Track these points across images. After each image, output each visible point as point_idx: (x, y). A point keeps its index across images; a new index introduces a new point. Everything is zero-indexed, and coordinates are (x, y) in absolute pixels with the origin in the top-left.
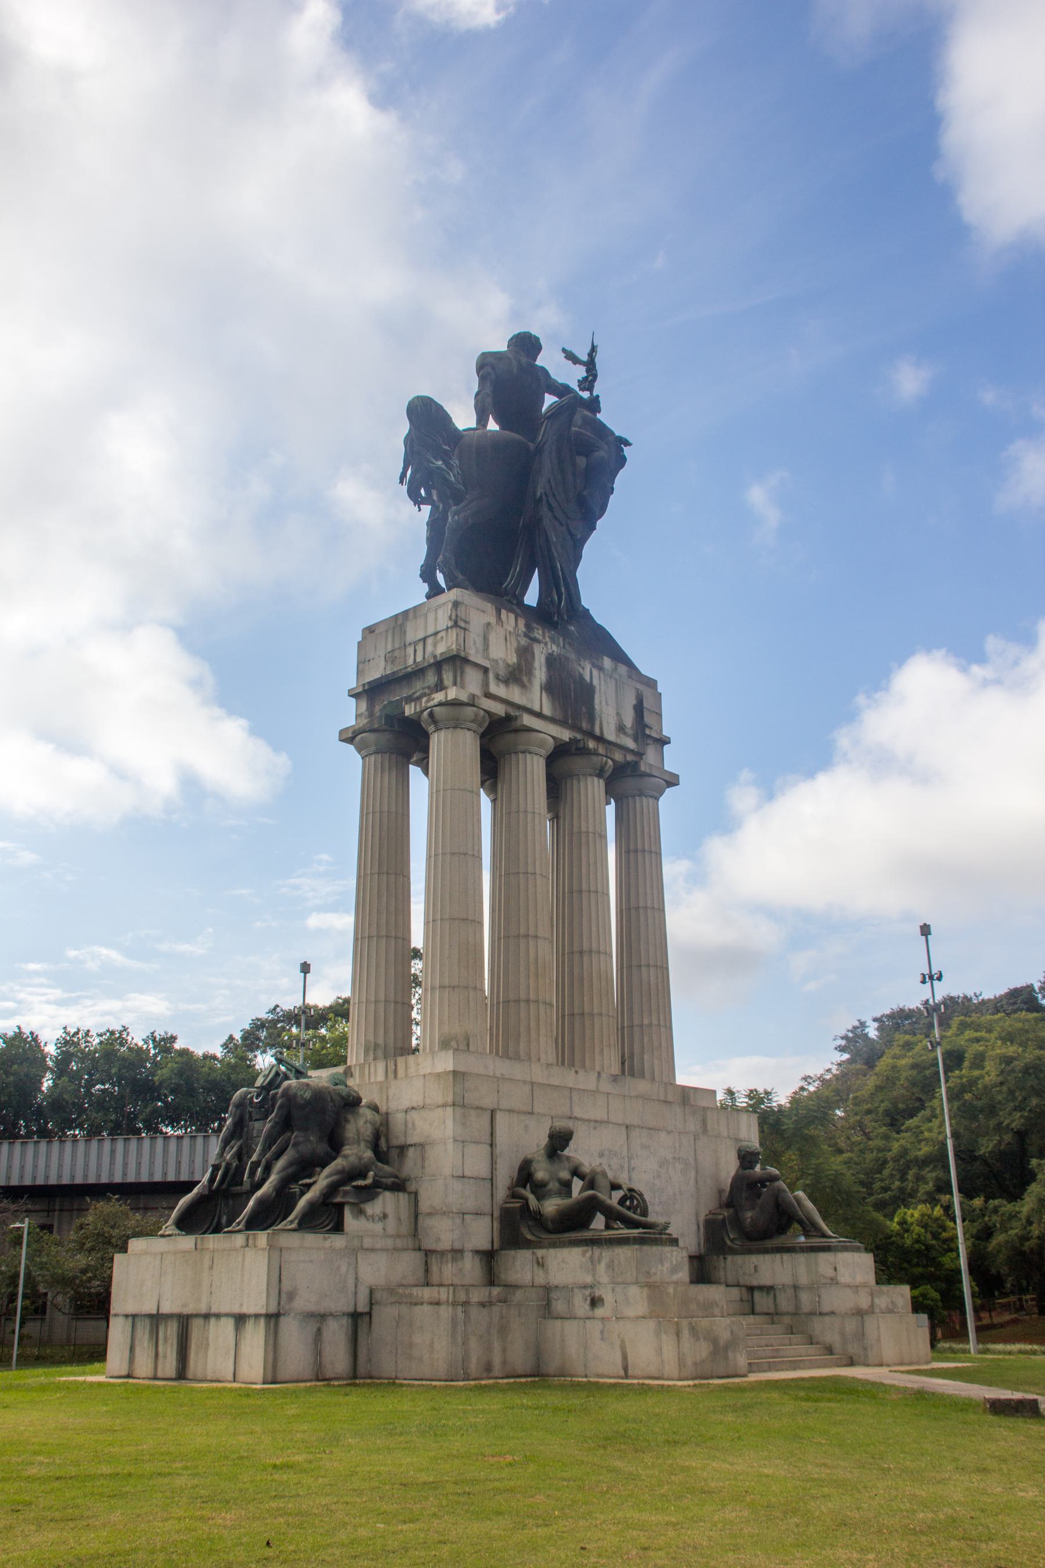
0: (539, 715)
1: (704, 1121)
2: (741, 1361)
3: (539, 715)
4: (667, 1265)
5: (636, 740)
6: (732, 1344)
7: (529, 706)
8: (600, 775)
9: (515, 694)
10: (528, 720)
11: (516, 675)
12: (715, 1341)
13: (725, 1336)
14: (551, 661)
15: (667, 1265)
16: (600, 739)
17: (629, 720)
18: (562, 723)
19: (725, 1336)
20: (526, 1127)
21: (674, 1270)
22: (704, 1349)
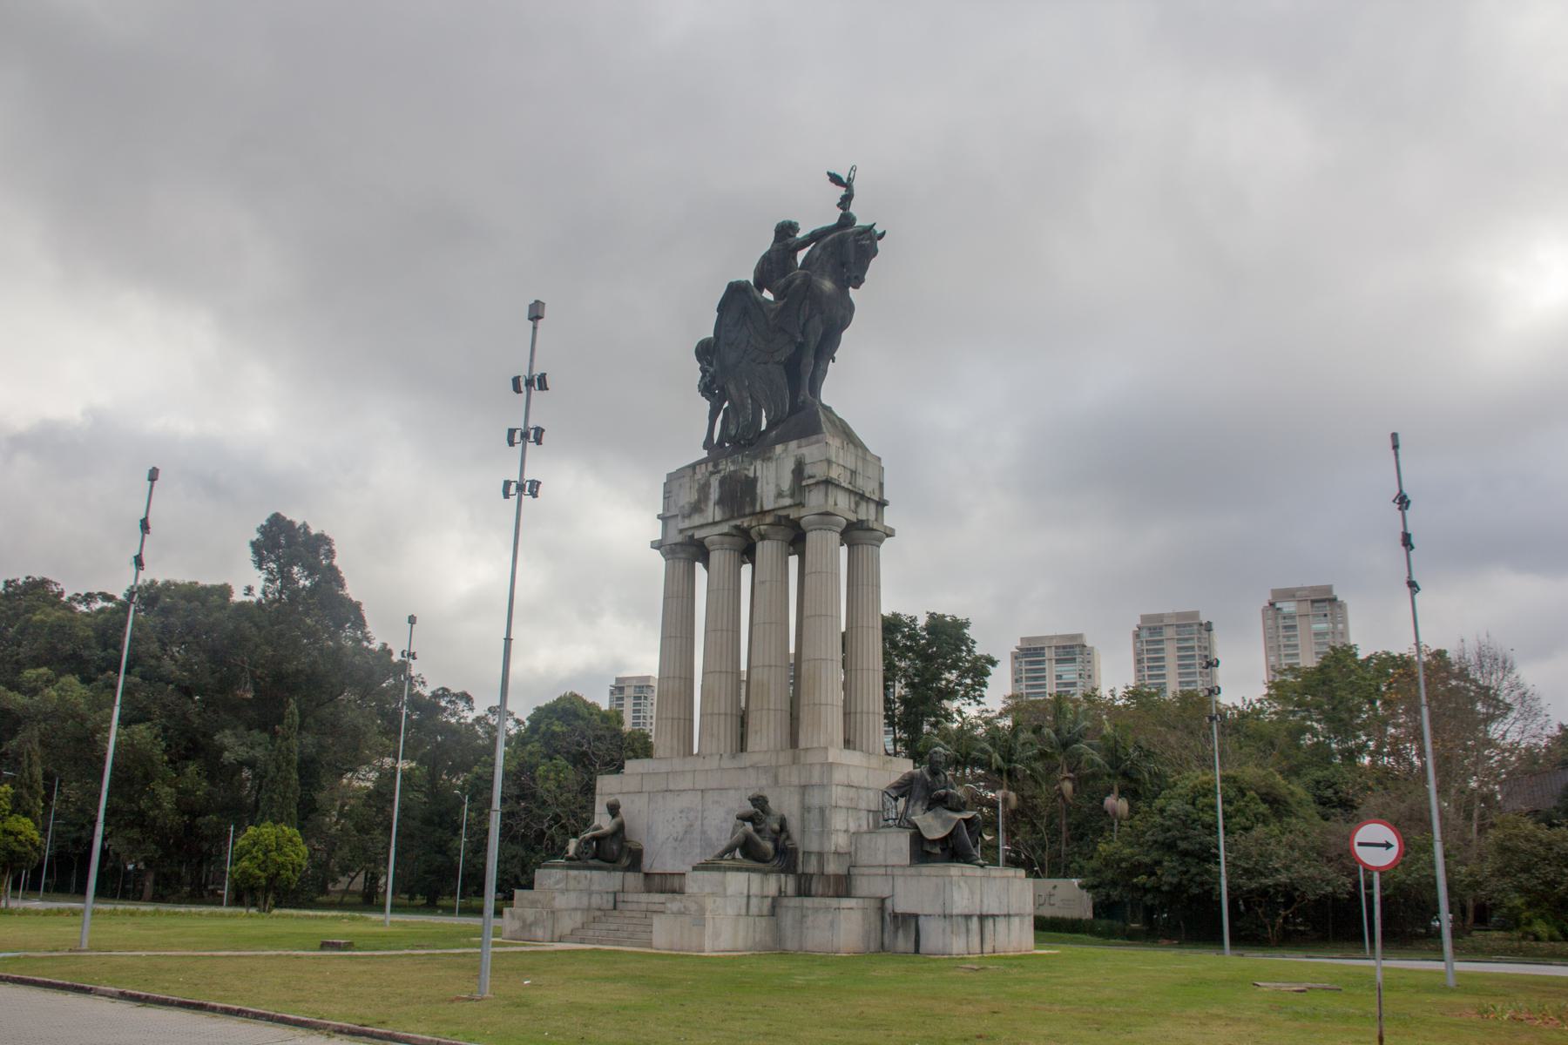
0: (715, 523)
1: (776, 777)
2: (539, 933)
3: (715, 523)
5: (792, 496)
6: (535, 923)
7: (702, 521)
8: (763, 537)
9: (697, 520)
10: (698, 534)
11: (697, 508)
12: (524, 921)
13: (531, 919)
14: (722, 483)
16: (764, 513)
17: (786, 484)
18: (732, 518)
19: (531, 919)
21: (557, 882)
22: (517, 925)
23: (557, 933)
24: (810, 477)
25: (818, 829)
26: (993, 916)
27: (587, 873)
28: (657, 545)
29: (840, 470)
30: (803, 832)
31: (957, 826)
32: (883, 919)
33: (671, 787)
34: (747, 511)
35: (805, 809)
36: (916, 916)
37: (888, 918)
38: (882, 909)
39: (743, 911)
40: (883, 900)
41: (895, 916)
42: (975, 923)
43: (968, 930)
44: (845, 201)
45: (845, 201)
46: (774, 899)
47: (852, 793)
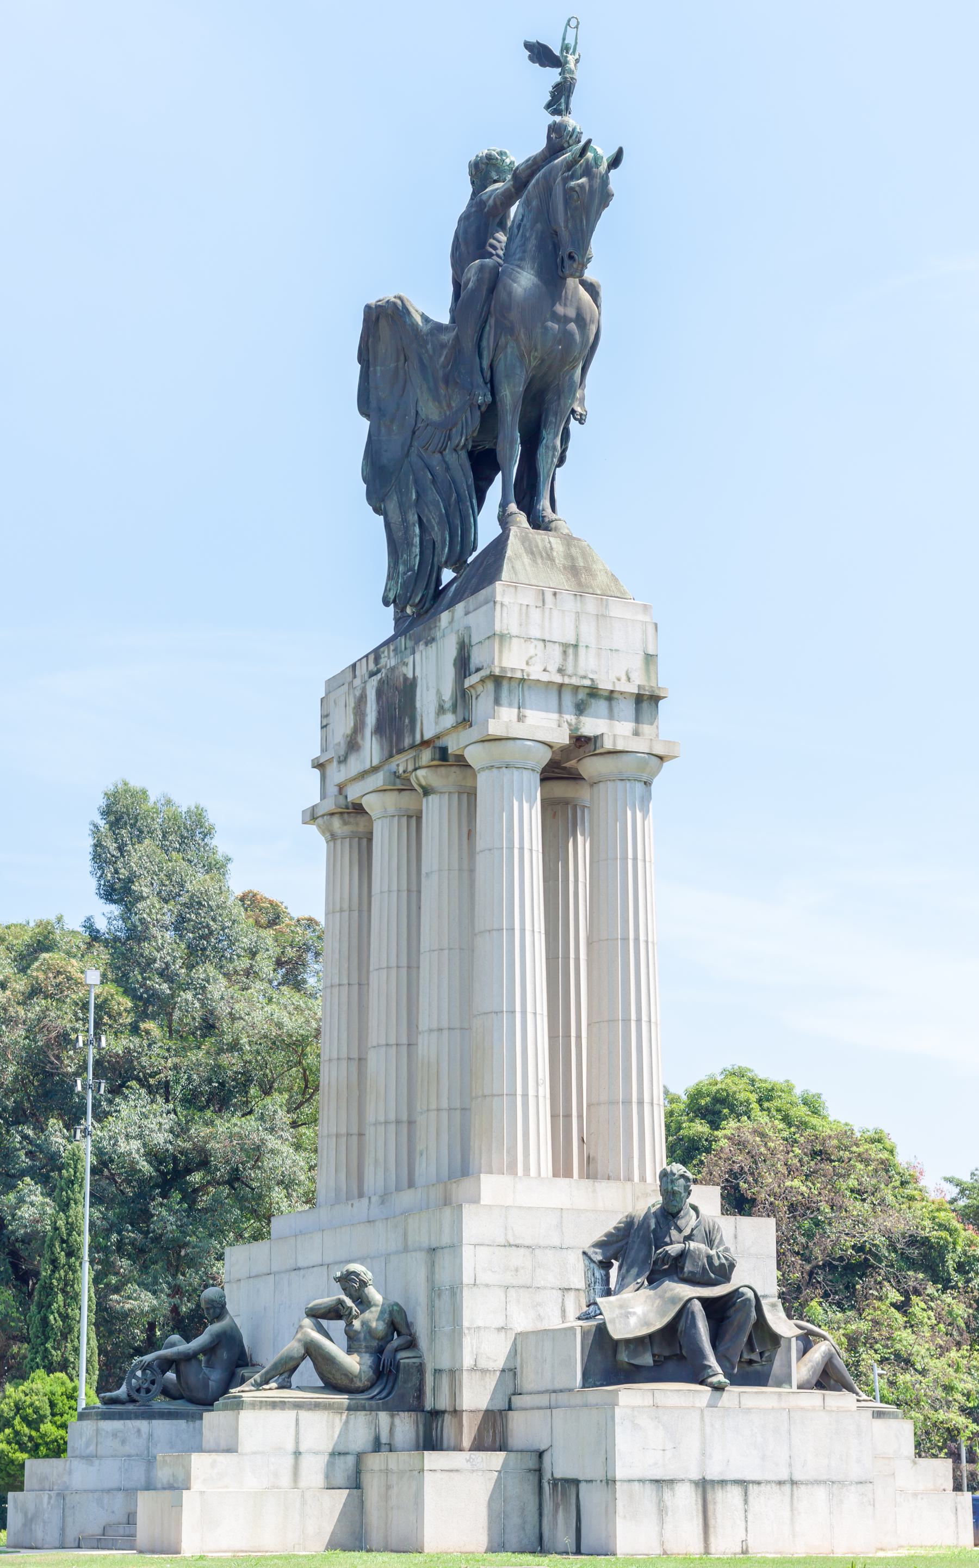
4: (84, 1439)
15: (84, 1439)
20: (258, 1291)
23: (72, 1534)
24: (478, 670)
25: (448, 1329)
26: (743, 1483)
27: (143, 1425)
28: (312, 816)
29: (533, 649)
30: (433, 1332)
31: (684, 1312)
32: (540, 1488)
33: (301, 1263)
34: (407, 742)
35: (434, 1291)
36: (576, 1482)
37: (546, 1487)
38: (539, 1471)
39: (285, 1480)
40: (541, 1454)
41: (555, 1482)
42: (684, 1499)
43: (662, 1510)
44: (560, 97)
45: (560, 97)
46: (359, 1456)
47: (518, 1257)
